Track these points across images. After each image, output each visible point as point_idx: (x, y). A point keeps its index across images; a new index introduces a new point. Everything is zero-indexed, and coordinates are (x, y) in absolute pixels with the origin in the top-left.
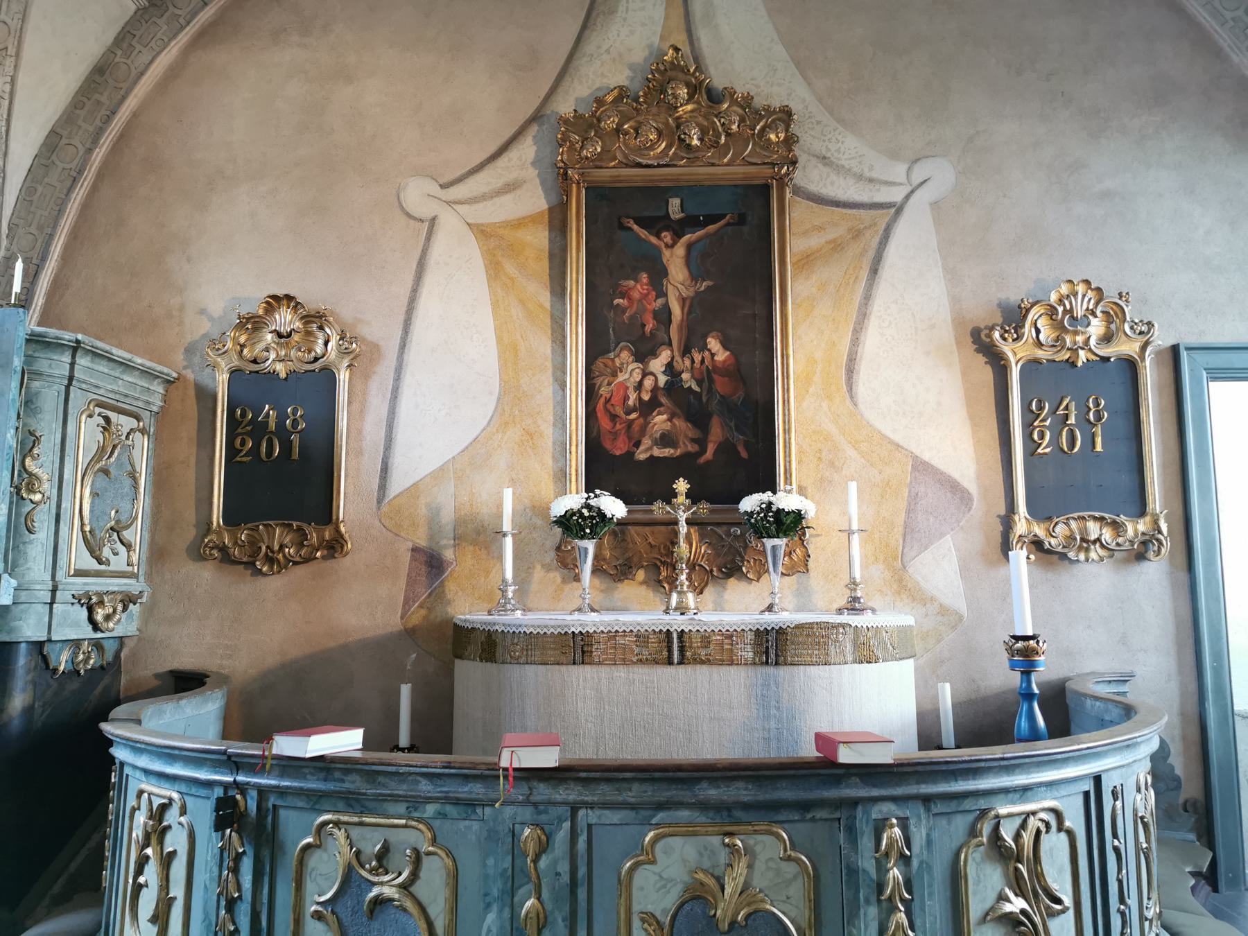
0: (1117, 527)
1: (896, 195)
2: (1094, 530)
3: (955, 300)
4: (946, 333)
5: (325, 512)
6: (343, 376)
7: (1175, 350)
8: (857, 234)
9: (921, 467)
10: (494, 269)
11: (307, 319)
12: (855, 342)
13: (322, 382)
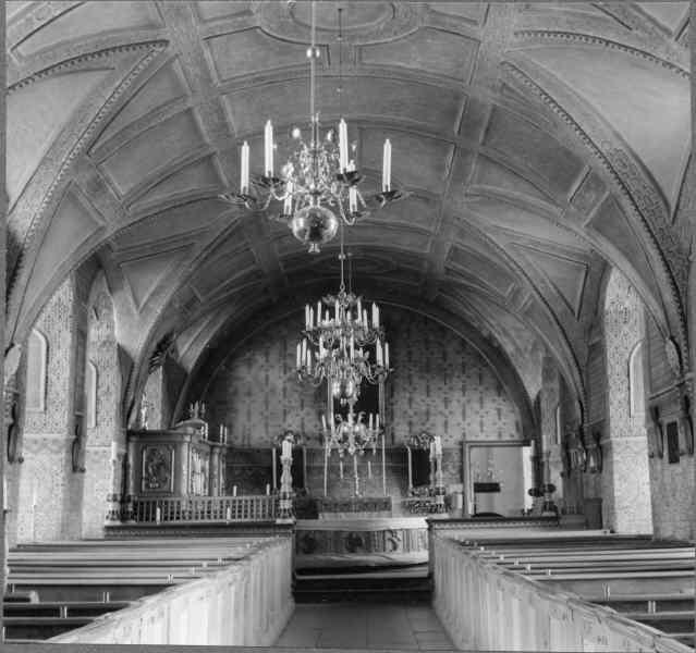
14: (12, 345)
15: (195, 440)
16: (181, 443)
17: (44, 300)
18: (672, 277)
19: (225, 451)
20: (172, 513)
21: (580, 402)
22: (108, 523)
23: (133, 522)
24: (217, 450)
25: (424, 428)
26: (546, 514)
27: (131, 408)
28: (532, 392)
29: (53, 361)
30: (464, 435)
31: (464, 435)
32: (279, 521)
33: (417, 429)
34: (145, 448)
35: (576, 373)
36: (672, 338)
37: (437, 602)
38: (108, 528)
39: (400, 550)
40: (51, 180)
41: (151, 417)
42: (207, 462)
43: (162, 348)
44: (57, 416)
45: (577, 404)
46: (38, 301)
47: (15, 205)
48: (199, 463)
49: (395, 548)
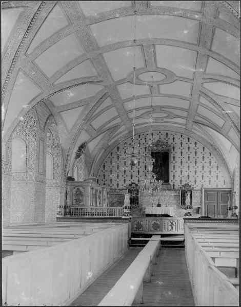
16: (88, 186)
19: (108, 190)
20: (80, 213)
22: (57, 216)
23: (69, 216)
24: (105, 189)
25: (187, 183)
26: (233, 218)
27: (68, 172)
29: (29, 153)
30: (202, 186)
31: (202, 186)
32: (123, 217)
33: (184, 183)
34: (74, 188)
37: (185, 250)
38: (57, 218)
39: (174, 229)
44: (32, 174)
49: (172, 228)
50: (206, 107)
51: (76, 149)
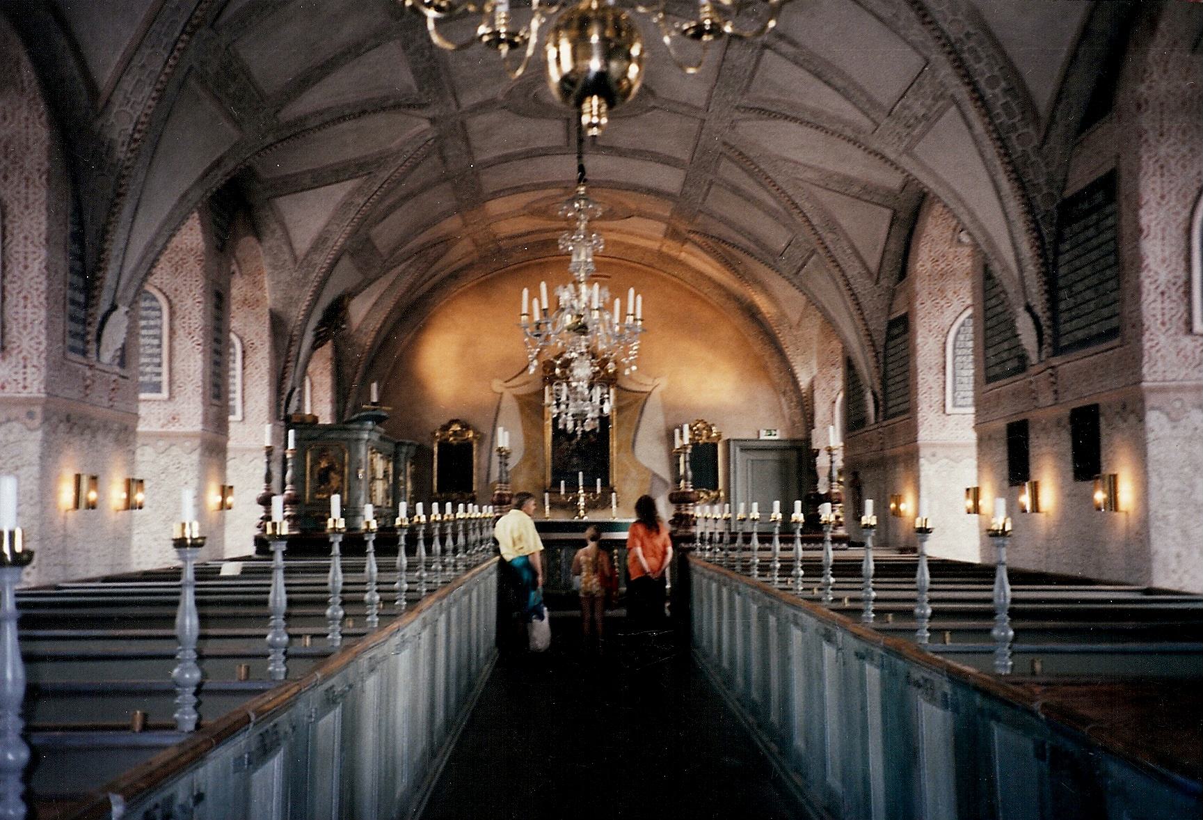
0: (708, 494)
1: (648, 389)
2: (702, 495)
3: (666, 422)
4: (663, 433)
5: (470, 490)
6: (475, 445)
7: (728, 441)
8: (636, 401)
9: (655, 475)
10: (522, 410)
11: (462, 427)
12: (635, 435)
13: (466, 448)
14: (114, 307)
15: (375, 437)
16: (358, 440)
17: (160, 243)
18: (1034, 221)
21: (874, 394)
24: (404, 450)
28: (804, 382)
35: (870, 355)
36: (1029, 309)
40: (155, 60)
41: (319, 403)
42: (391, 465)
43: (334, 318)
45: (869, 397)
46: (152, 244)
47: (108, 101)
48: (380, 465)
50: (736, 190)
51: (317, 316)
